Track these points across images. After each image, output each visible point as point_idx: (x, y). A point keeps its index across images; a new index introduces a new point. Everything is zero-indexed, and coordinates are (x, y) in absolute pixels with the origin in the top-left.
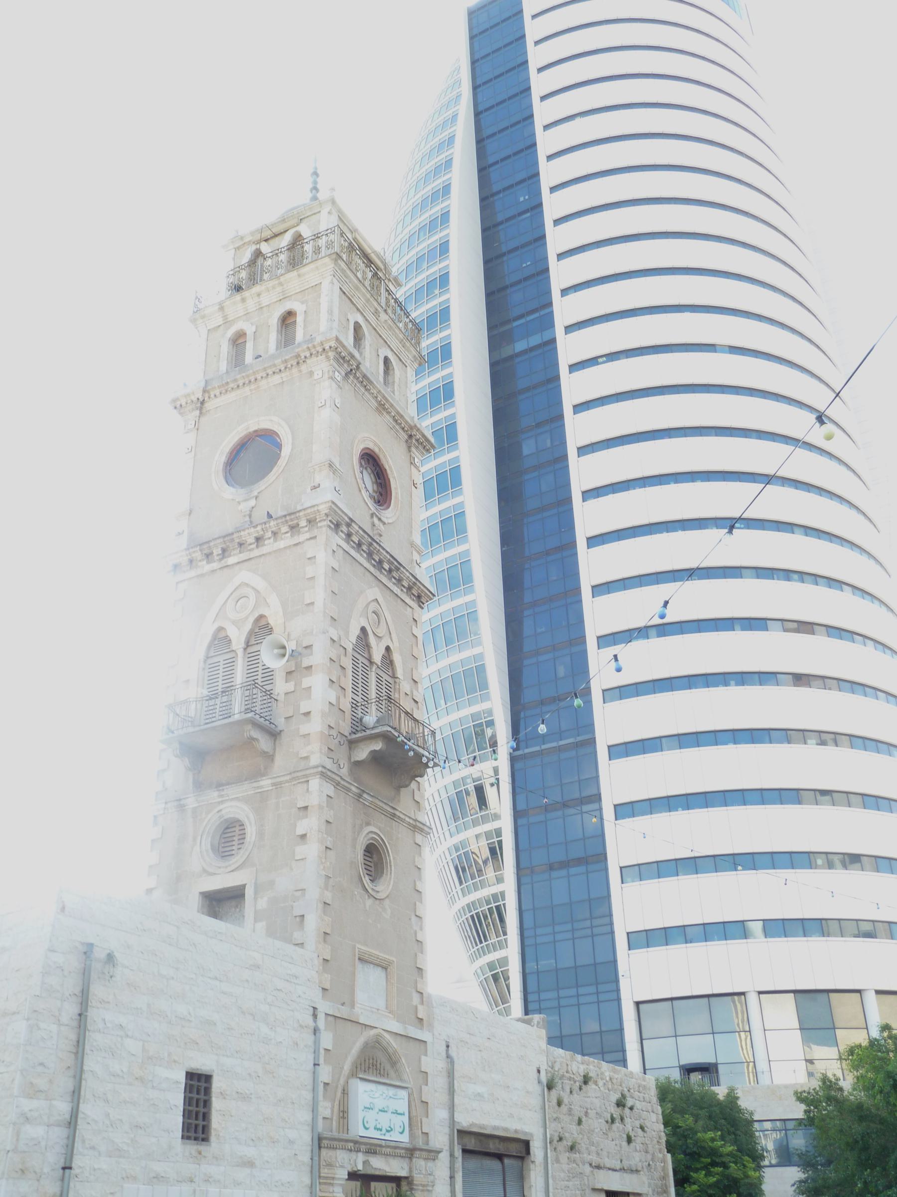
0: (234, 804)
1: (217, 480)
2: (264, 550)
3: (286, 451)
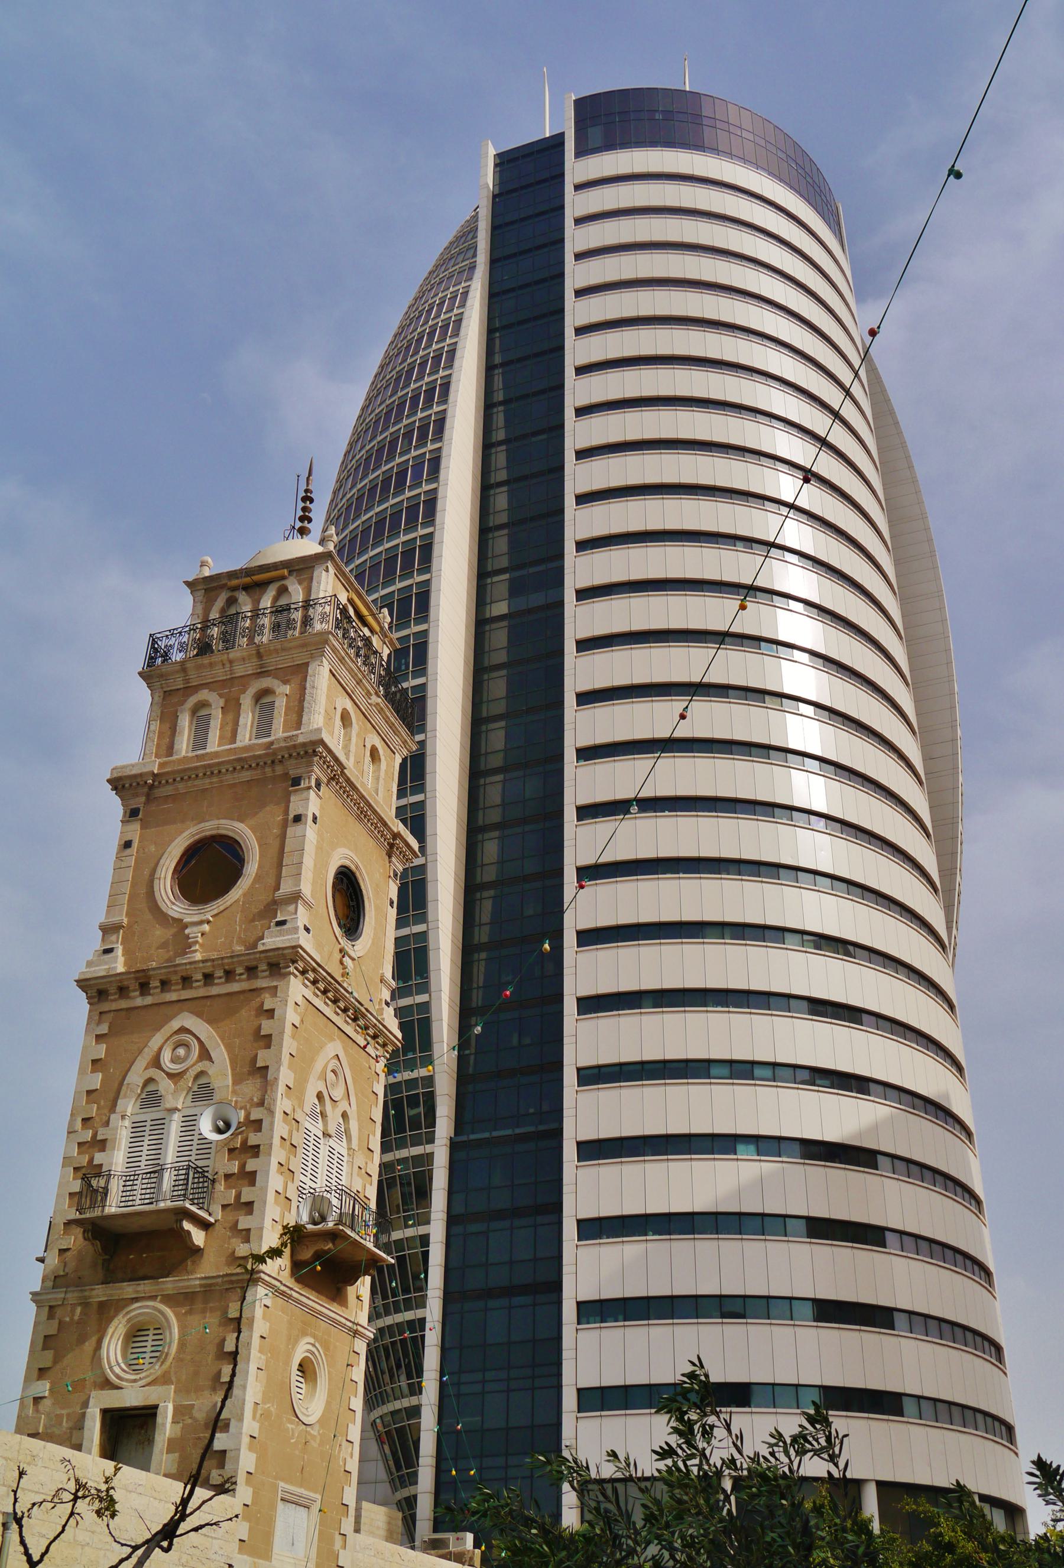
2: (214, 990)
3: (251, 868)
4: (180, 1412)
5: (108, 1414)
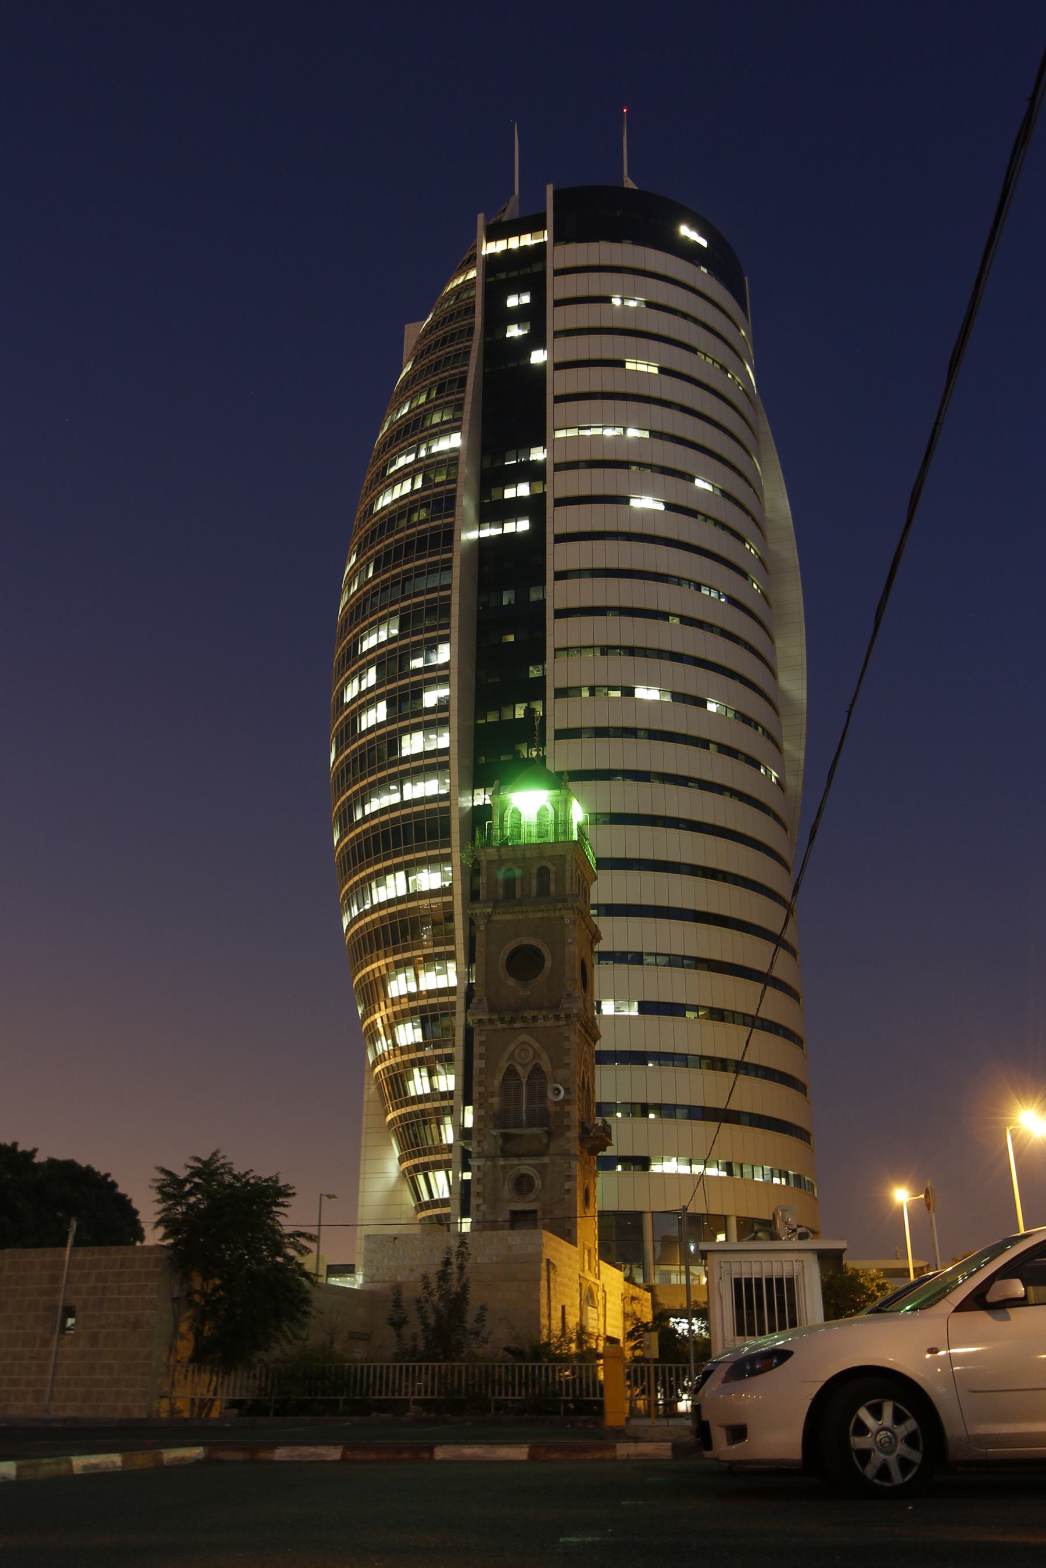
0: (525, 1166)
1: (502, 972)
3: (548, 964)
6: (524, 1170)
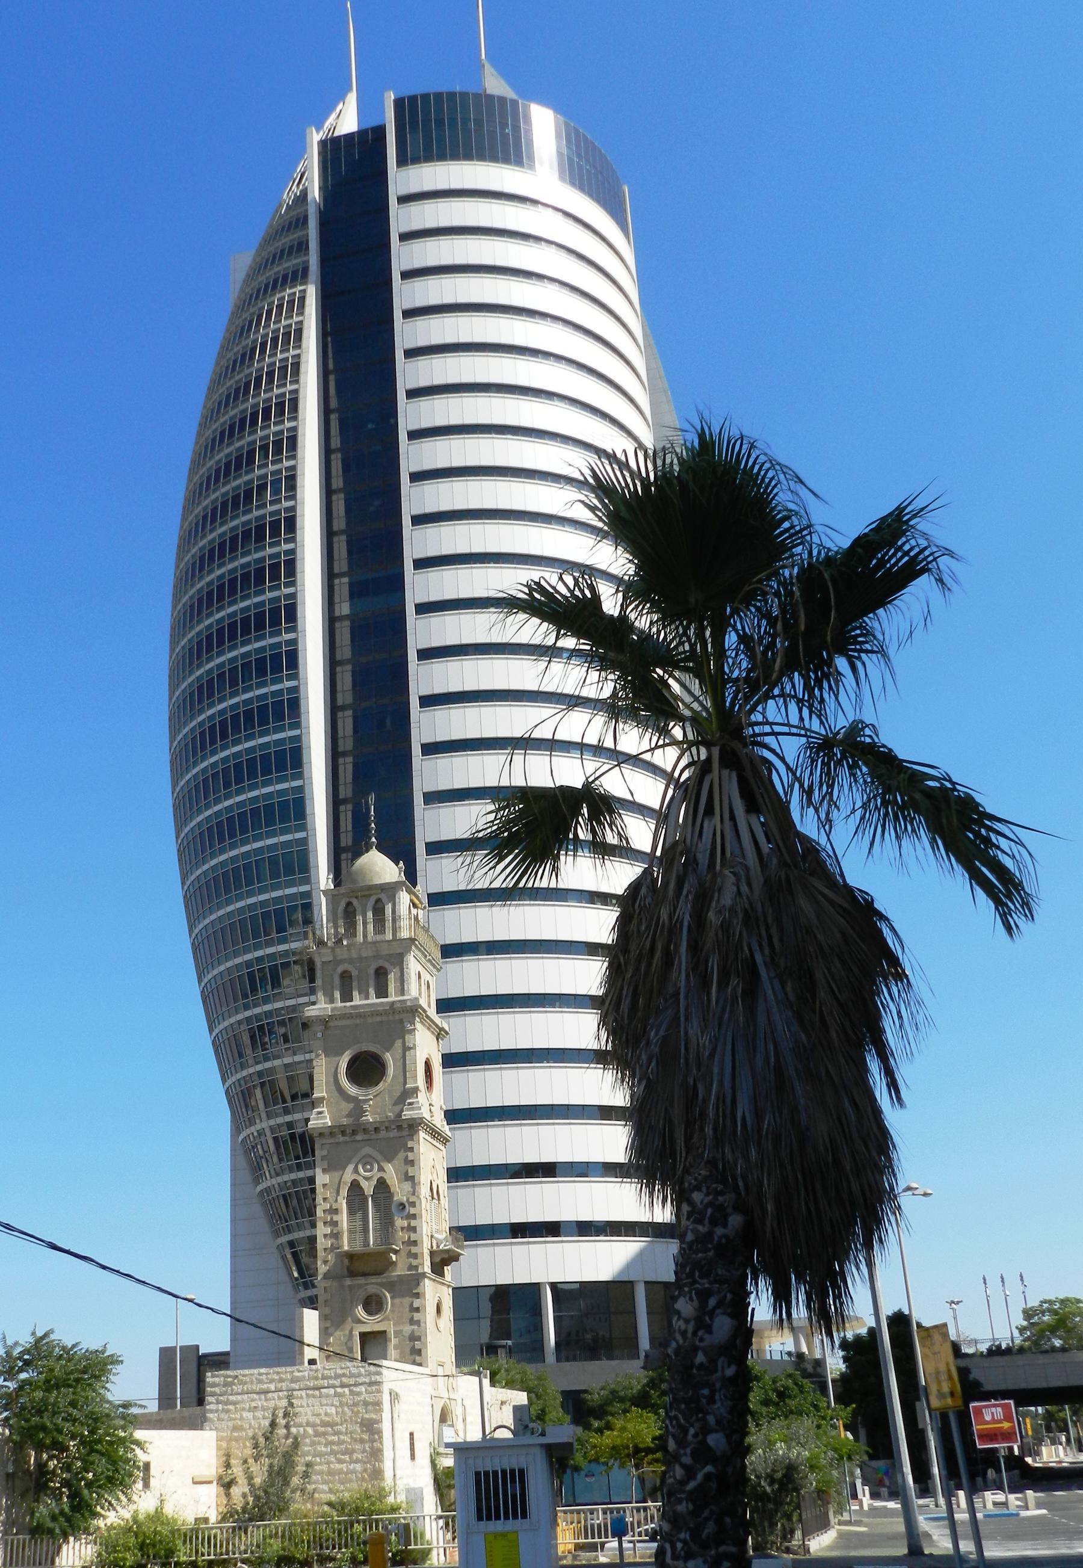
3: (391, 1071)
4: (397, 1333)
5: (363, 1335)
6: (372, 1290)
